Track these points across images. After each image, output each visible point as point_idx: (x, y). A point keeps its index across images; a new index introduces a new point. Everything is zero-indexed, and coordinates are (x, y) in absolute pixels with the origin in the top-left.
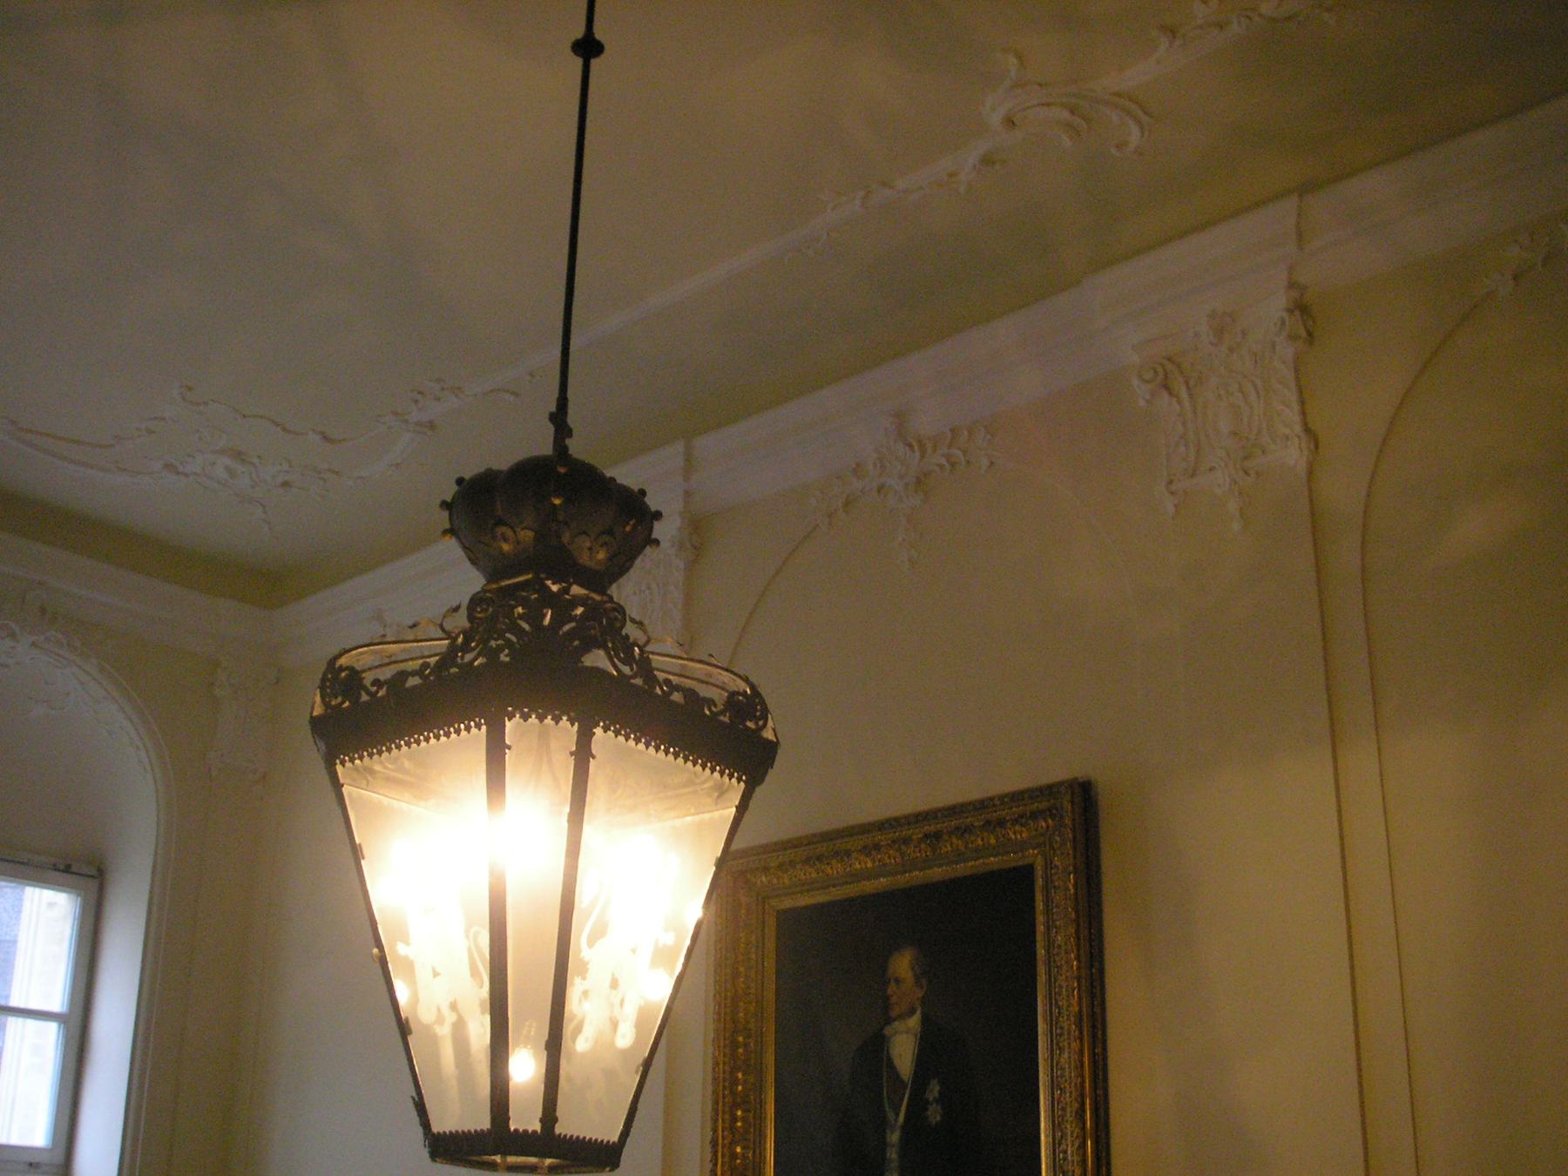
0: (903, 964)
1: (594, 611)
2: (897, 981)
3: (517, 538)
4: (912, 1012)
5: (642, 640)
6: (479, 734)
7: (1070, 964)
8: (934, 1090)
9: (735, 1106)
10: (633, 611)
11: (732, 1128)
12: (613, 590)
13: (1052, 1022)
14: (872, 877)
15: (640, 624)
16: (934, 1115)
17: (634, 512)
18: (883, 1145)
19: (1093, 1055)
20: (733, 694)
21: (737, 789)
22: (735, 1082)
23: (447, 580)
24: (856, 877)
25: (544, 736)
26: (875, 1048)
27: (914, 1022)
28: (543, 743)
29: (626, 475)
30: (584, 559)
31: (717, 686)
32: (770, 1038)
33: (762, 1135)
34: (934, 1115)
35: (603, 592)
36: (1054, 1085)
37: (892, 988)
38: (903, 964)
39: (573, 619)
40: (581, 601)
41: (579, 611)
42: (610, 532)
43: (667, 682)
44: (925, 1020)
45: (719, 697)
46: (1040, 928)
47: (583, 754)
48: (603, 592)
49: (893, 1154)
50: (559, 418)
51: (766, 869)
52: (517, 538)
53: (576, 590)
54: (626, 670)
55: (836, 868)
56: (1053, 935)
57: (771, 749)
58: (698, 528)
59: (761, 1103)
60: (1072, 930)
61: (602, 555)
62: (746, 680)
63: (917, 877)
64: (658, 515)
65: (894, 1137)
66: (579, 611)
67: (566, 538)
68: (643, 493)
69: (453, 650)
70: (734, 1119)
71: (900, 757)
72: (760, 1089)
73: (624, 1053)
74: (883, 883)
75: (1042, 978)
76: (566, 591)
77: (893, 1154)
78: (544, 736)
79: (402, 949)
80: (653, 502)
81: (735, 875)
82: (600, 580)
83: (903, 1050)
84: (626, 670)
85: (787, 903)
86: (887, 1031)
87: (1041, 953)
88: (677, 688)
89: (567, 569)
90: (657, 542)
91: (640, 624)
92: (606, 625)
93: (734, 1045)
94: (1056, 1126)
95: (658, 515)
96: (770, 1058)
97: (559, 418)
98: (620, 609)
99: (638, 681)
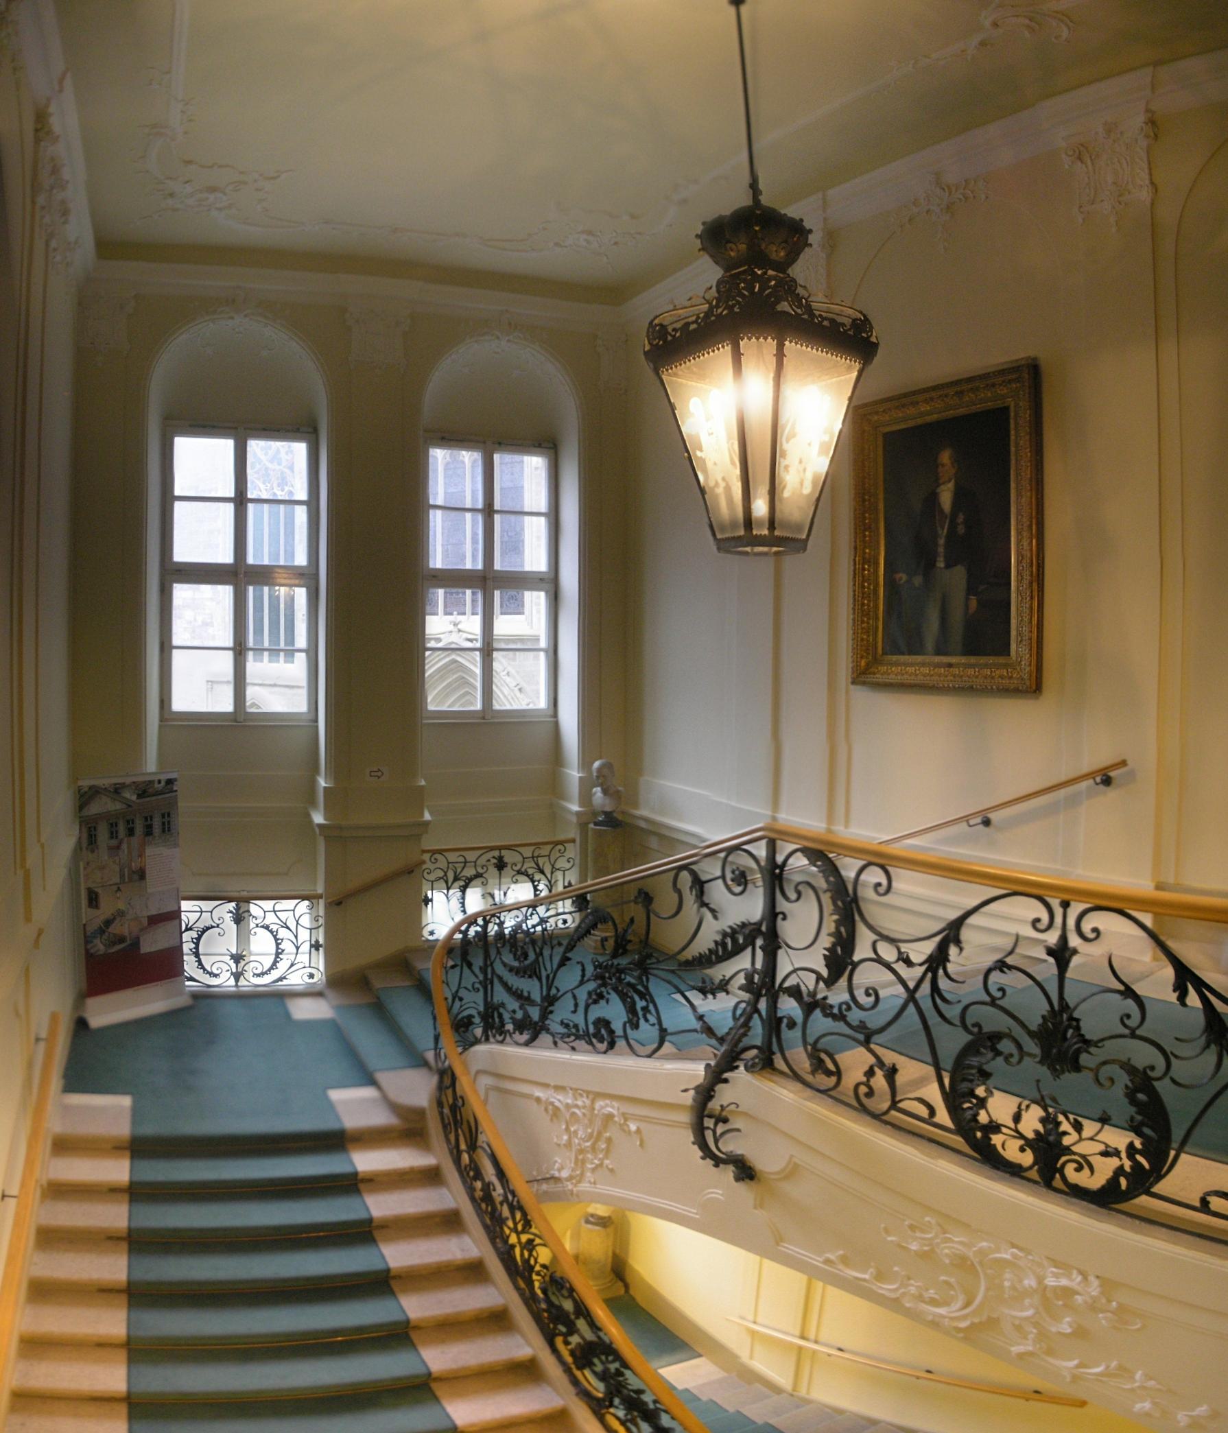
0: (946, 457)
1: (780, 282)
2: (943, 465)
3: (738, 248)
4: (950, 481)
5: (806, 295)
6: (728, 348)
7: (1026, 454)
8: (961, 518)
9: (865, 530)
10: (800, 281)
11: (864, 541)
12: (790, 271)
13: (1017, 484)
14: (929, 412)
15: (805, 287)
16: (961, 530)
17: (796, 233)
18: (936, 545)
19: (1037, 499)
20: (854, 320)
21: (857, 366)
22: (865, 518)
23: (706, 275)
24: (922, 415)
25: (760, 347)
26: (933, 498)
27: (951, 485)
28: (758, 351)
29: (792, 212)
30: (774, 256)
31: (846, 315)
32: (881, 496)
33: (878, 542)
34: (961, 530)
35: (784, 272)
36: (1019, 513)
37: (940, 469)
38: (946, 457)
39: (770, 287)
40: (774, 278)
41: (773, 283)
42: (786, 242)
43: (821, 316)
44: (956, 484)
45: (847, 321)
46: (1013, 438)
47: (780, 355)
48: (784, 272)
49: (941, 550)
50: (754, 186)
51: (877, 413)
52: (738, 248)
53: (770, 272)
54: (799, 311)
55: (911, 411)
56: (1019, 440)
57: (875, 346)
58: (832, 238)
59: (878, 529)
60: (1028, 437)
61: (782, 254)
62: (861, 313)
63: (951, 413)
64: (810, 231)
65: (942, 541)
66: (773, 283)
67: (763, 246)
68: (802, 220)
69: (711, 308)
70: (865, 536)
71: (940, 352)
72: (877, 521)
73: (809, 496)
74: (935, 417)
75: (1013, 462)
76: (765, 273)
77: (941, 550)
78: (760, 347)
79: (699, 454)
80: (807, 225)
81: (861, 415)
82: (782, 267)
83: (946, 498)
84: (799, 311)
85: (888, 429)
86: (938, 490)
87: (1013, 449)
88: (826, 319)
89: (765, 262)
90: (811, 245)
91: (805, 287)
92: (789, 288)
93: (864, 500)
94: (1019, 533)
95: (810, 231)
96: (881, 506)
97: (754, 186)
98: (794, 280)
99: (806, 317)
